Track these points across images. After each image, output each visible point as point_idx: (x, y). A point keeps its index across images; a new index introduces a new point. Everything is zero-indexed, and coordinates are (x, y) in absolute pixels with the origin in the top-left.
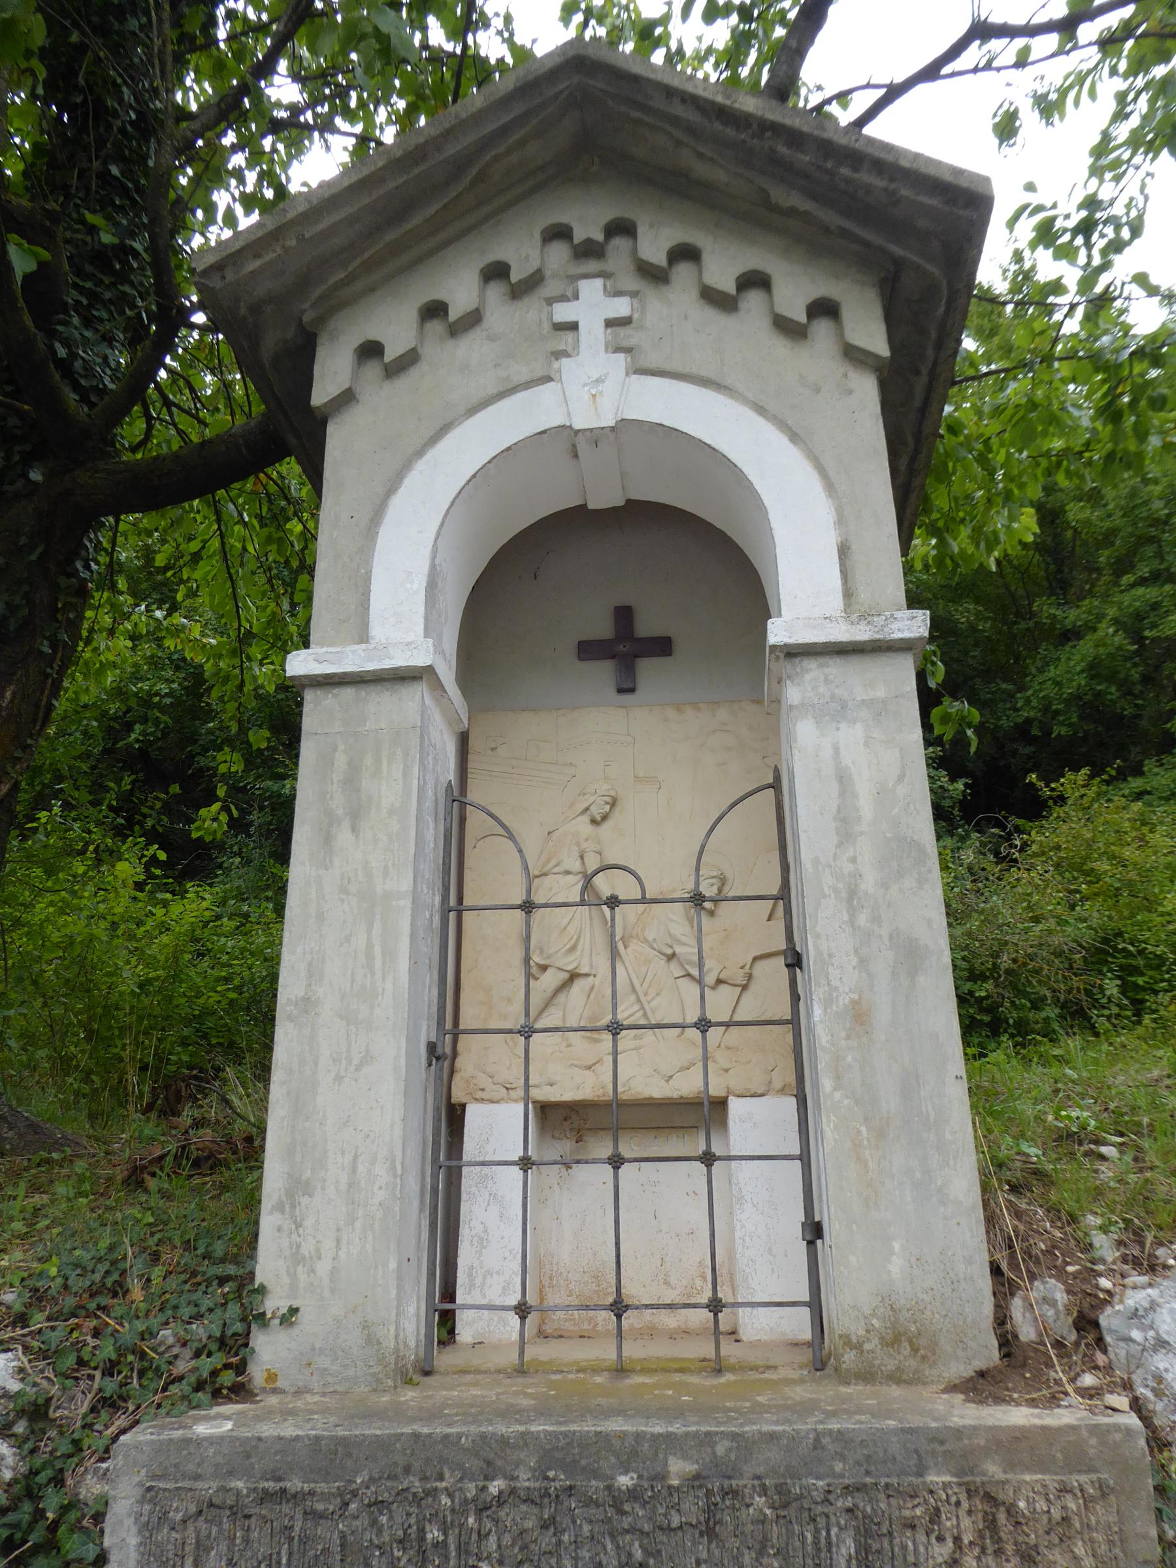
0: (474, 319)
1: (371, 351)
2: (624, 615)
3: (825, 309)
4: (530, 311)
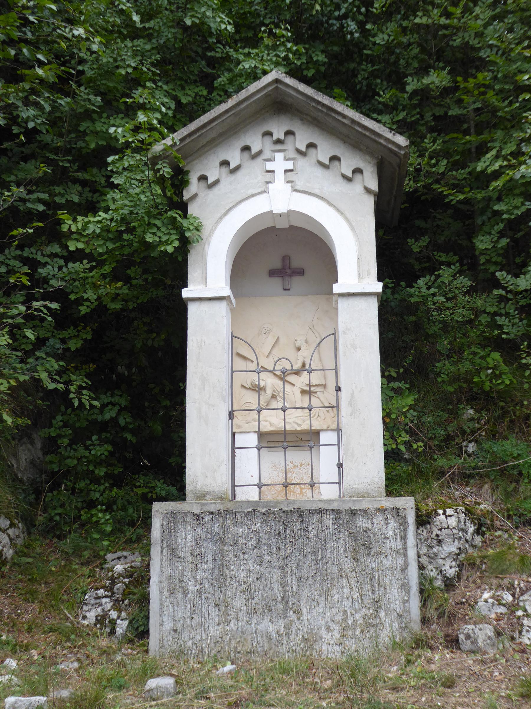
1: (203, 178)
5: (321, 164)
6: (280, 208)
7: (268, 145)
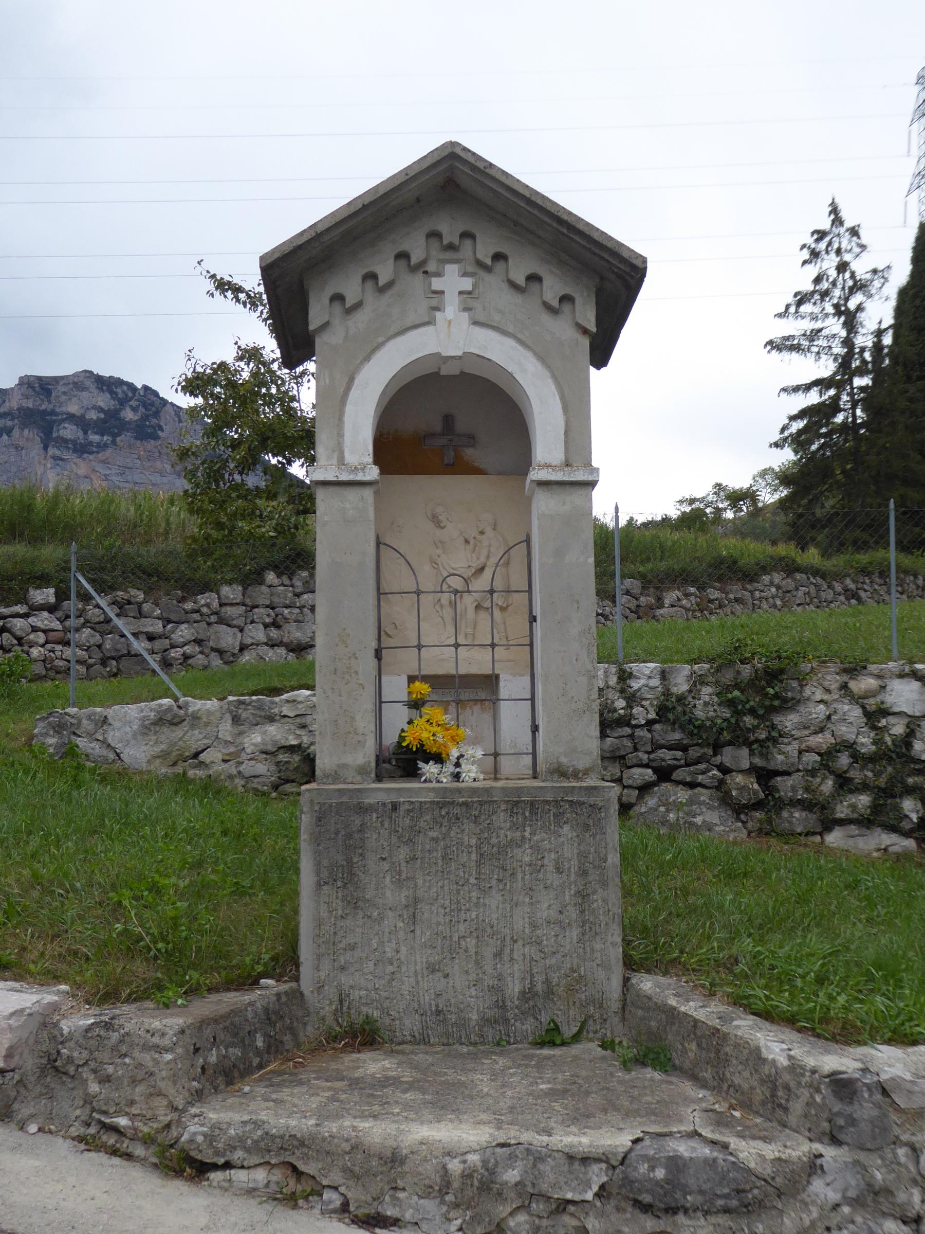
1: (338, 298)
3: (566, 299)
5: (513, 285)
6: (453, 350)
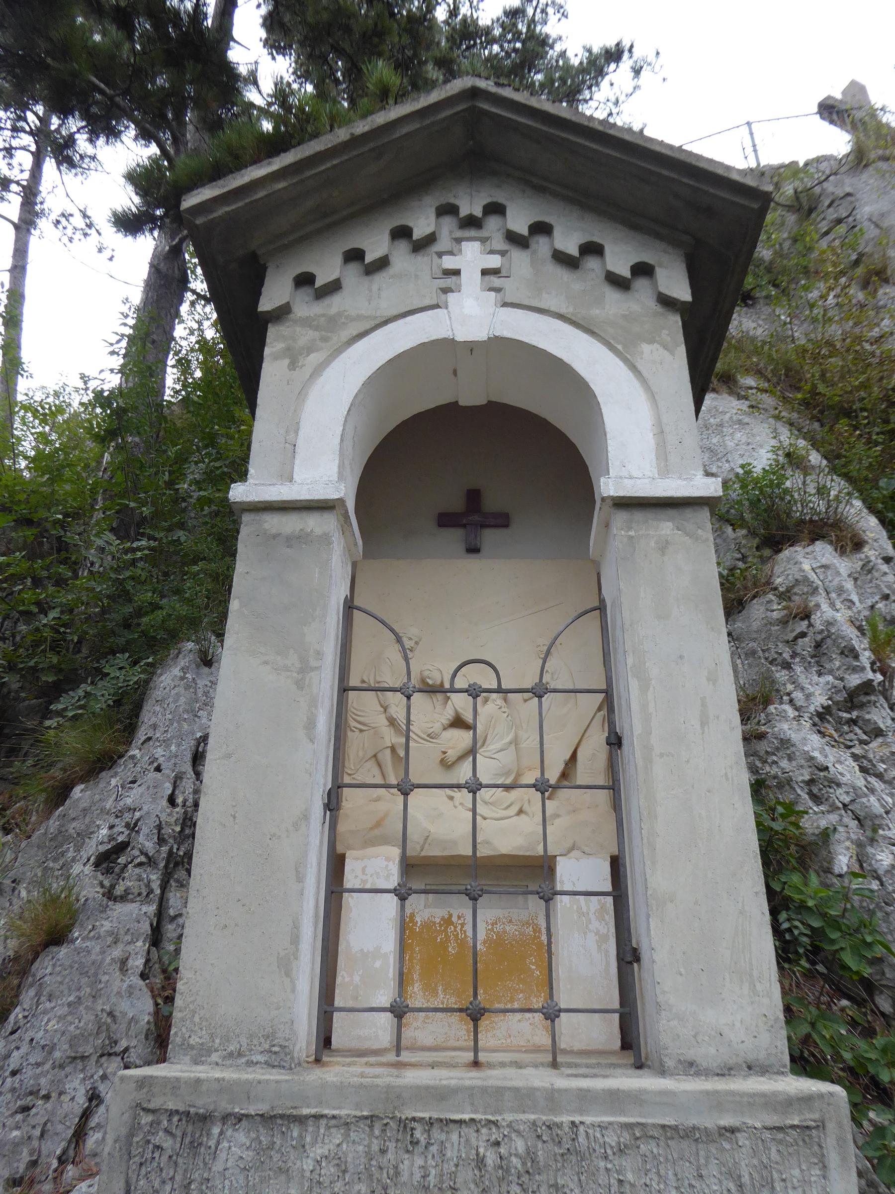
0: (383, 263)
1: (304, 280)
2: (474, 497)
3: (643, 270)
4: (423, 263)
5: (561, 259)
7: (448, 225)
